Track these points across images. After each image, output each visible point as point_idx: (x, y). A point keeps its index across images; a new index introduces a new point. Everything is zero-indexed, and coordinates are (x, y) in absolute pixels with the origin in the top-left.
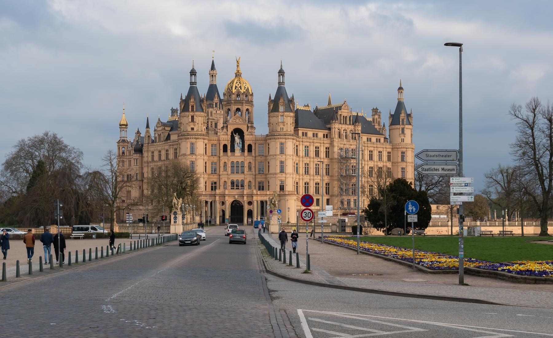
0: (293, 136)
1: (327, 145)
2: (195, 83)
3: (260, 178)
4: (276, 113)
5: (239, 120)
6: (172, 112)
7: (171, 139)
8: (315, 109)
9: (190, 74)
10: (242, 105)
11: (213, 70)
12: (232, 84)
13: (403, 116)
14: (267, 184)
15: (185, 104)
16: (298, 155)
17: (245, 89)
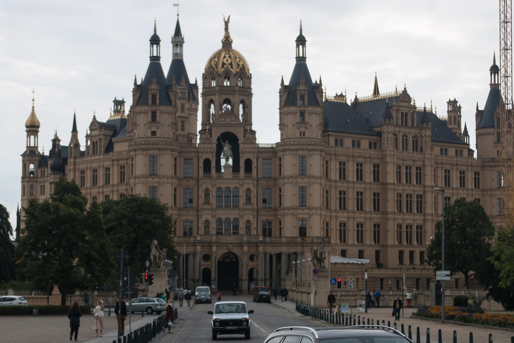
0: (321, 146)
1: (376, 161)
3: (264, 217)
4: (293, 109)
5: (230, 118)
6: (114, 106)
7: (114, 151)
8: (353, 100)
9: (149, 42)
11: (179, 37)
12: (216, 59)
14: (278, 226)
15: (141, 92)
16: (329, 177)
17: (238, 68)
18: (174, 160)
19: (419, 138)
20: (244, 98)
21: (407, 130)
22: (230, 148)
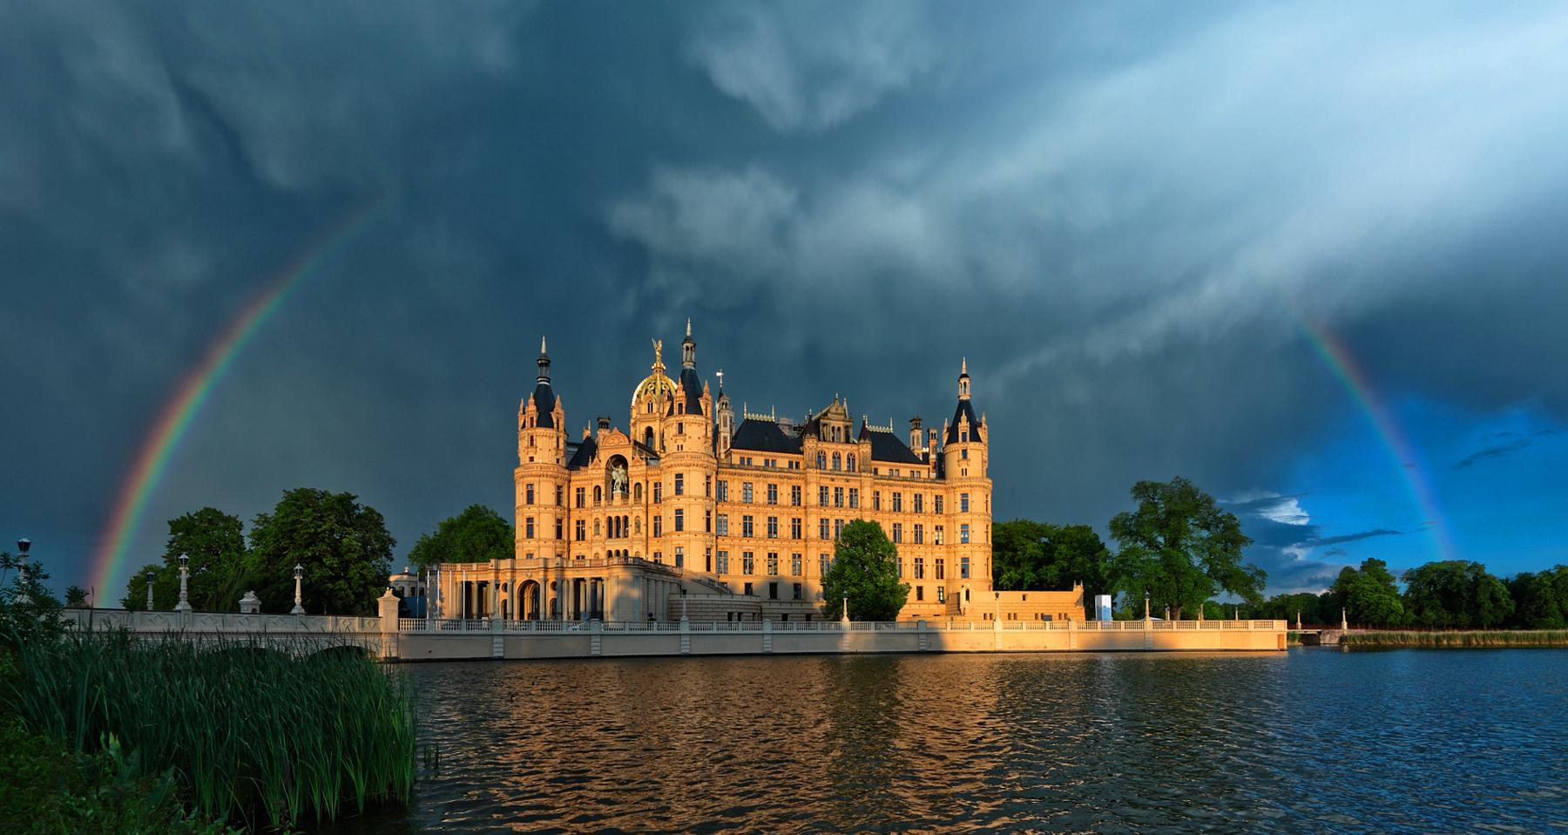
13: (964, 425)
19: (857, 456)
21: (840, 447)
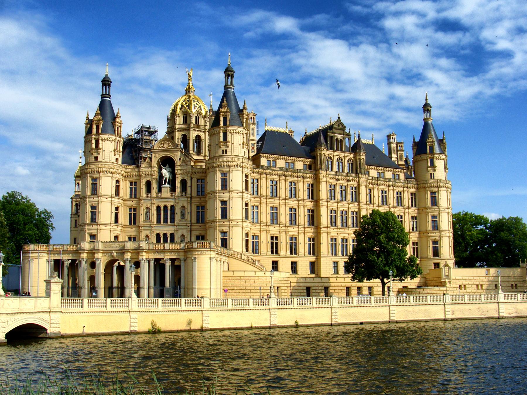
1: (311, 181)
2: (109, 96)
5: (168, 144)
10: (189, 130)
17: (195, 108)
18: (114, 182)
20: (202, 134)
21: (342, 154)
22: (170, 171)
